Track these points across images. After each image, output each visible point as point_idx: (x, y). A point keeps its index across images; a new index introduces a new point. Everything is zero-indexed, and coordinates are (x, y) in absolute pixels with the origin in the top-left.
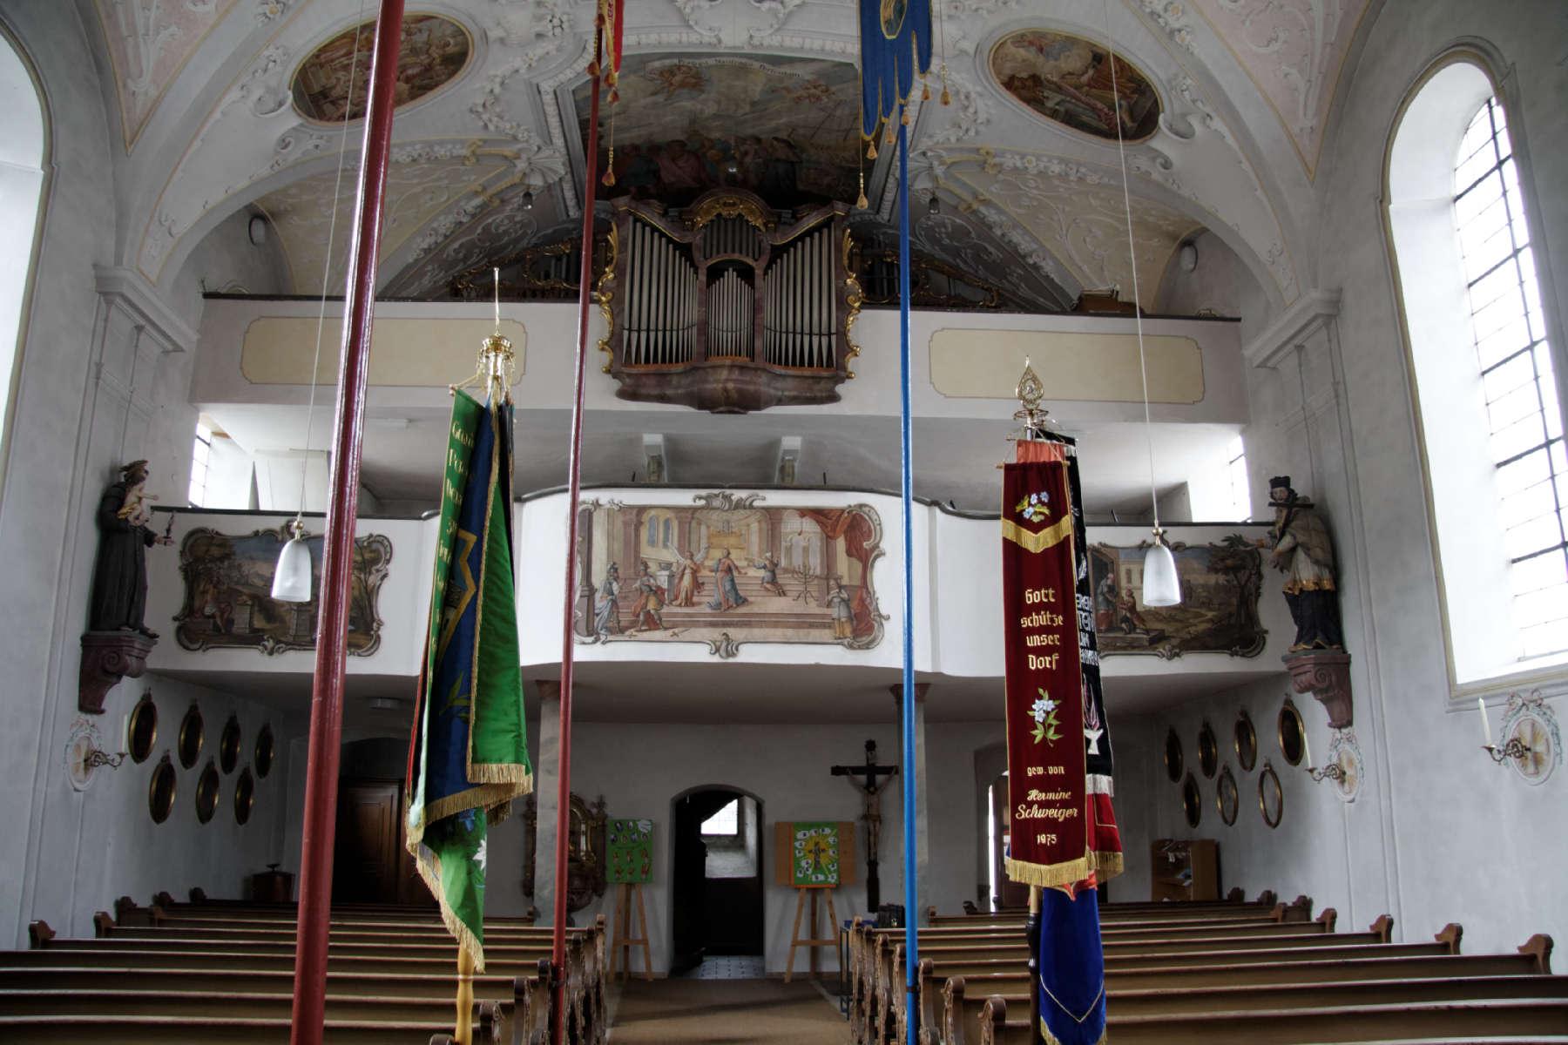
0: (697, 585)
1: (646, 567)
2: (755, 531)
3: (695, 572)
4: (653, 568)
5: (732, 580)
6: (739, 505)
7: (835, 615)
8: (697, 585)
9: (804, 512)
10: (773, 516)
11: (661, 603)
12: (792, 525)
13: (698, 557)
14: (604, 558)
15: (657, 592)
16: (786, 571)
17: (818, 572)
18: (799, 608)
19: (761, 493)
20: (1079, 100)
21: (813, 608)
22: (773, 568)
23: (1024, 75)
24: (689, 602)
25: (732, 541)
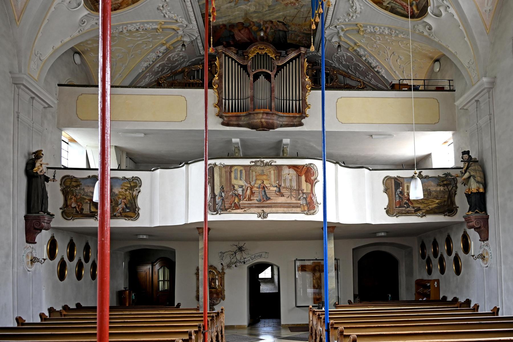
0: (252, 193)
3: (251, 189)
4: (236, 187)
5: (265, 191)
6: (267, 164)
9: (290, 167)
10: (279, 168)
11: (240, 200)
12: (286, 171)
13: (252, 183)
14: (219, 184)
15: (238, 196)
16: (284, 188)
17: (295, 188)
18: (289, 201)
19: (274, 160)
21: (294, 201)
22: (279, 187)
24: (249, 199)
25: (265, 177)
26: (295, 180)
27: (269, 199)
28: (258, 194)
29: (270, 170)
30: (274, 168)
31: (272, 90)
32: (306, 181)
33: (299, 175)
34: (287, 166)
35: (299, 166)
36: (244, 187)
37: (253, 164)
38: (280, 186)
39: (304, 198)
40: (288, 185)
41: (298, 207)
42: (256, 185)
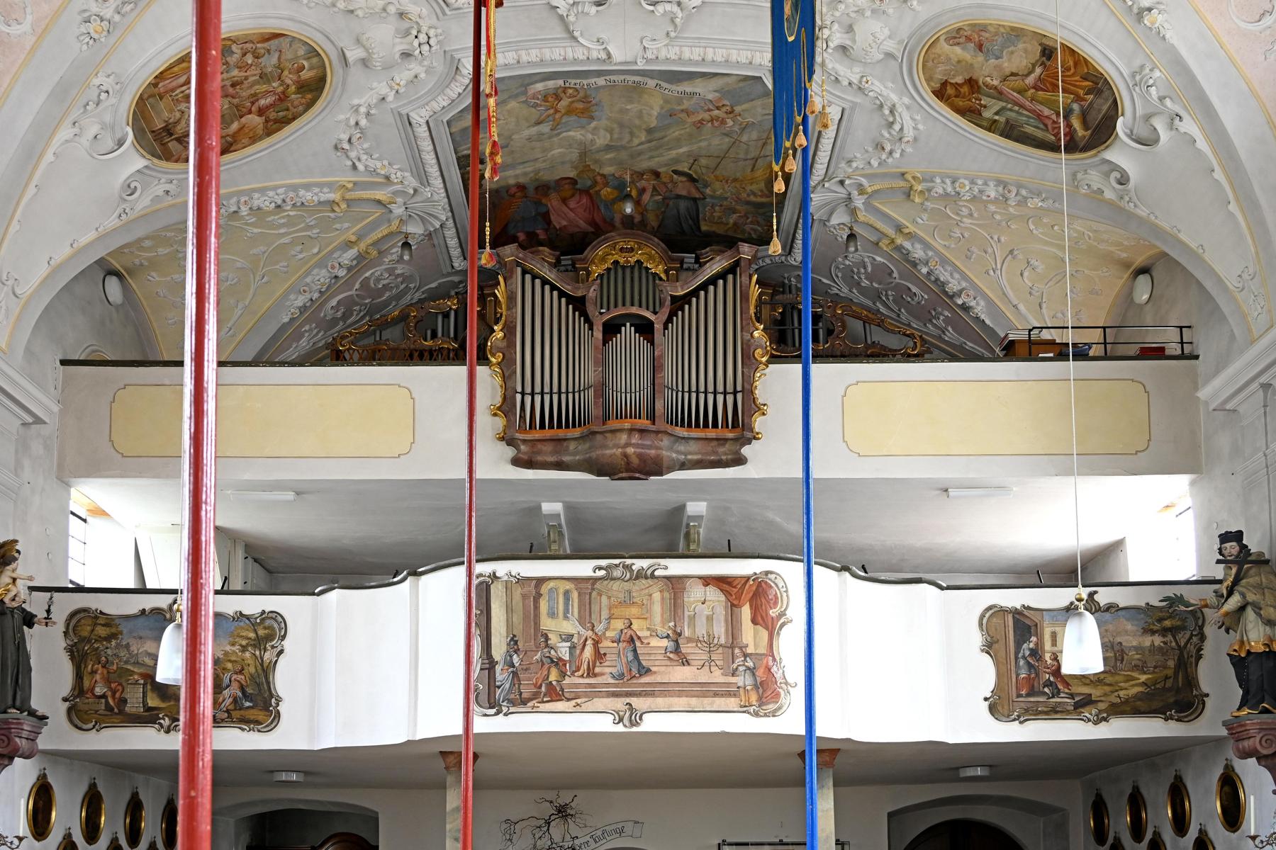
0: (599, 656)
1: (547, 639)
2: (658, 600)
3: (596, 644)
4: (553, 639)
5: (635, 650)
6: (641, 575)
7: (741, 684)
8: (599, 656)
9: (707, 580)
10: (676, 584)
11: (563, 675)
12: (695, 593)
13: (599, 628)
14: (503, 630)
15: (558, 663)
16: (689, 640)
17: (723, 641)
18: (703, 677)
19: (663, 562)
20: (1021, 106)
21: (717, 676)
22: (676, 638)
23: (959, 80)
24: (591, 673)
25: (634, 611)
26: (722, 618)
27: (648, 671)
28: (614, 657)
29: (651, 590)
30: (661, 584)
31: (656, 367)
32: (754, 621)
33: (733, 605)
34: (700, 578)
35: (736, 578)
36: (575, 640)
37: (603, 573)
38: (680, 635)
39: (749, 668)
40: (701, 631)
41: (729, 694)
42: (608, 634)
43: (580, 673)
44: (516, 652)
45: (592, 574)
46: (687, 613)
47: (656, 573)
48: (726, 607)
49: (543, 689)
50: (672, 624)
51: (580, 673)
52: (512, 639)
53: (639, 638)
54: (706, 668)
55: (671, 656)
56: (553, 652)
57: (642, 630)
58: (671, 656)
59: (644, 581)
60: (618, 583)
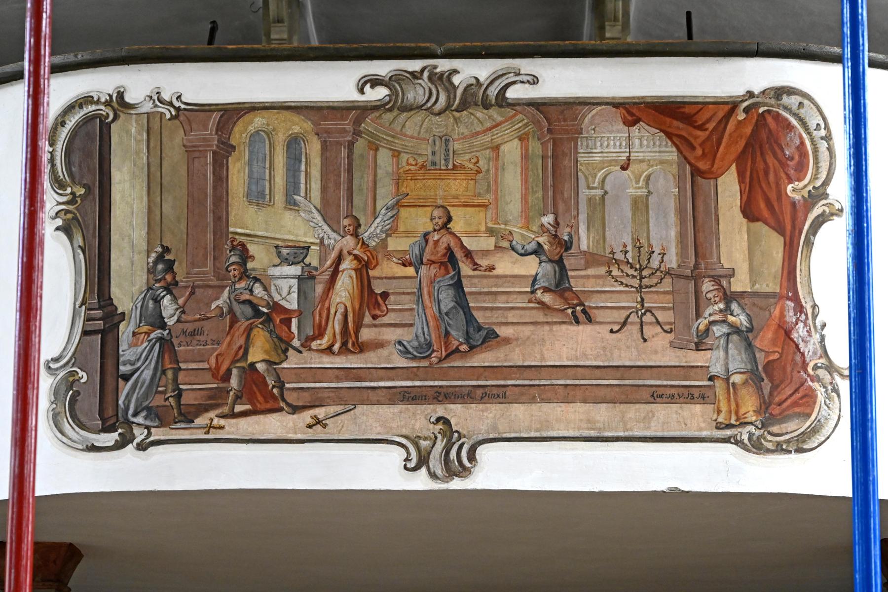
0: (370, 299)
1: (245, 256)
3: (364, 267)
4: (261, 257)
5: (458, 286)
6: (473, 98)
9: (634, 111)
10: (559, 121)
11: (283, 346)
13: (372, 230)
14: (140, 235)
15: (273, 317)
16: (591, 259)
17: (672, 261)
18: (626, 351)
19: (526, 65)
21: (660, 351)
24: (350, 342)
25: (457, 186)
26: (671, 205)
28: (408, 302)
29: (498, 135)
30: (521, 120)
32: (749, 212)
33: (696, 172)
34: (616, 104)
36: (313, 259)
37: (380, 93)
38: (567, 246)
39: (736, 330)
40: (619, 236)
42: (393, 244)
43: (324, 342)
44: (168, 289)
45: (356, 96)
46: (584, 193)
47: (511, 94)
48: (680, 178)
49: (234, 382)
50: (548, 219)
51: (324, 342)
52: (160, 258)
53: (468, 254)
54: (633, 329)
55: (547, 298)
56: (258, 290)
57: (475, 234)
58: (547, 298)
59: (480, 114)
60: (418, 117)
